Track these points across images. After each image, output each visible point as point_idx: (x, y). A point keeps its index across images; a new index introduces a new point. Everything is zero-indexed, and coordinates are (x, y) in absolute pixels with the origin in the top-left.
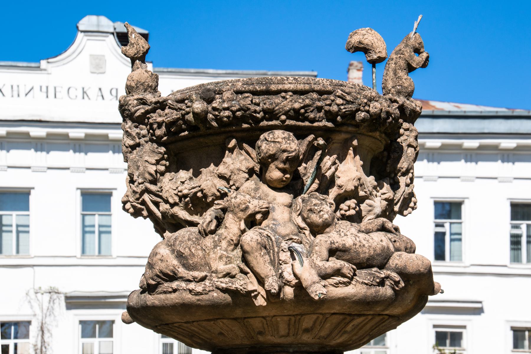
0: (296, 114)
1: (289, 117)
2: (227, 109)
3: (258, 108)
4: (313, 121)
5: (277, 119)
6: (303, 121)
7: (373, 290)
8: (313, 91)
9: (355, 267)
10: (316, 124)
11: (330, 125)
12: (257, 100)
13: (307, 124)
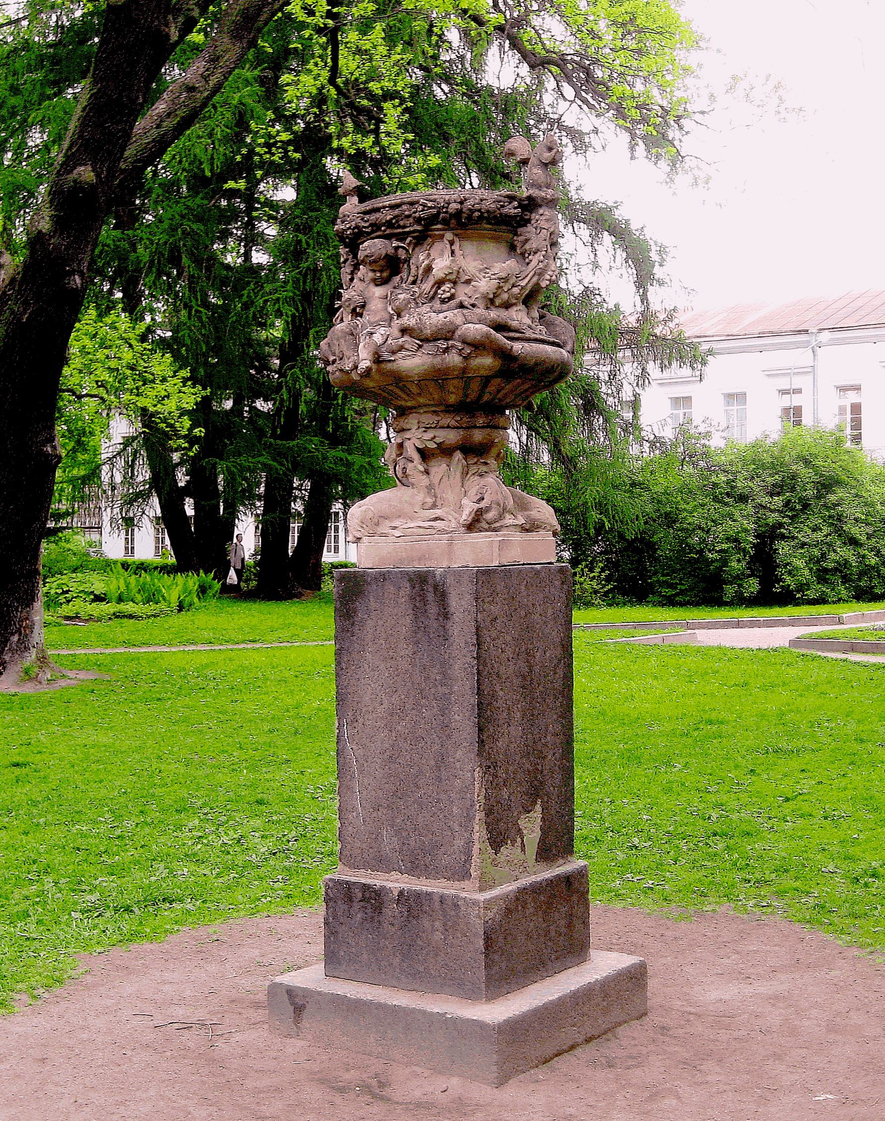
0: (389, 224)
1: (388, 227)
2: (349, 228)
3: (366, 225)
4: (405, 227)
5: (380, 230)
6: (397, 228)
7: (438, 360)
8: (404, 204)
9: (417, 342)
10: (407, 230)
11: (419, 228)
12: (367, 217)
13: (399, 230)
